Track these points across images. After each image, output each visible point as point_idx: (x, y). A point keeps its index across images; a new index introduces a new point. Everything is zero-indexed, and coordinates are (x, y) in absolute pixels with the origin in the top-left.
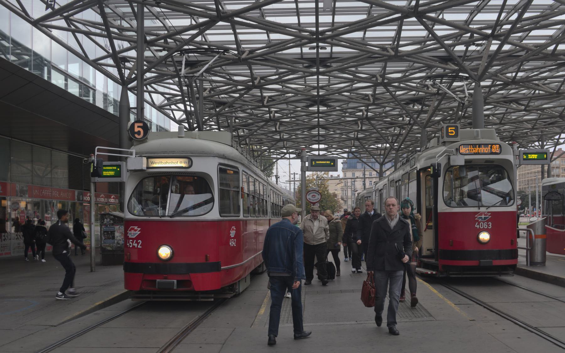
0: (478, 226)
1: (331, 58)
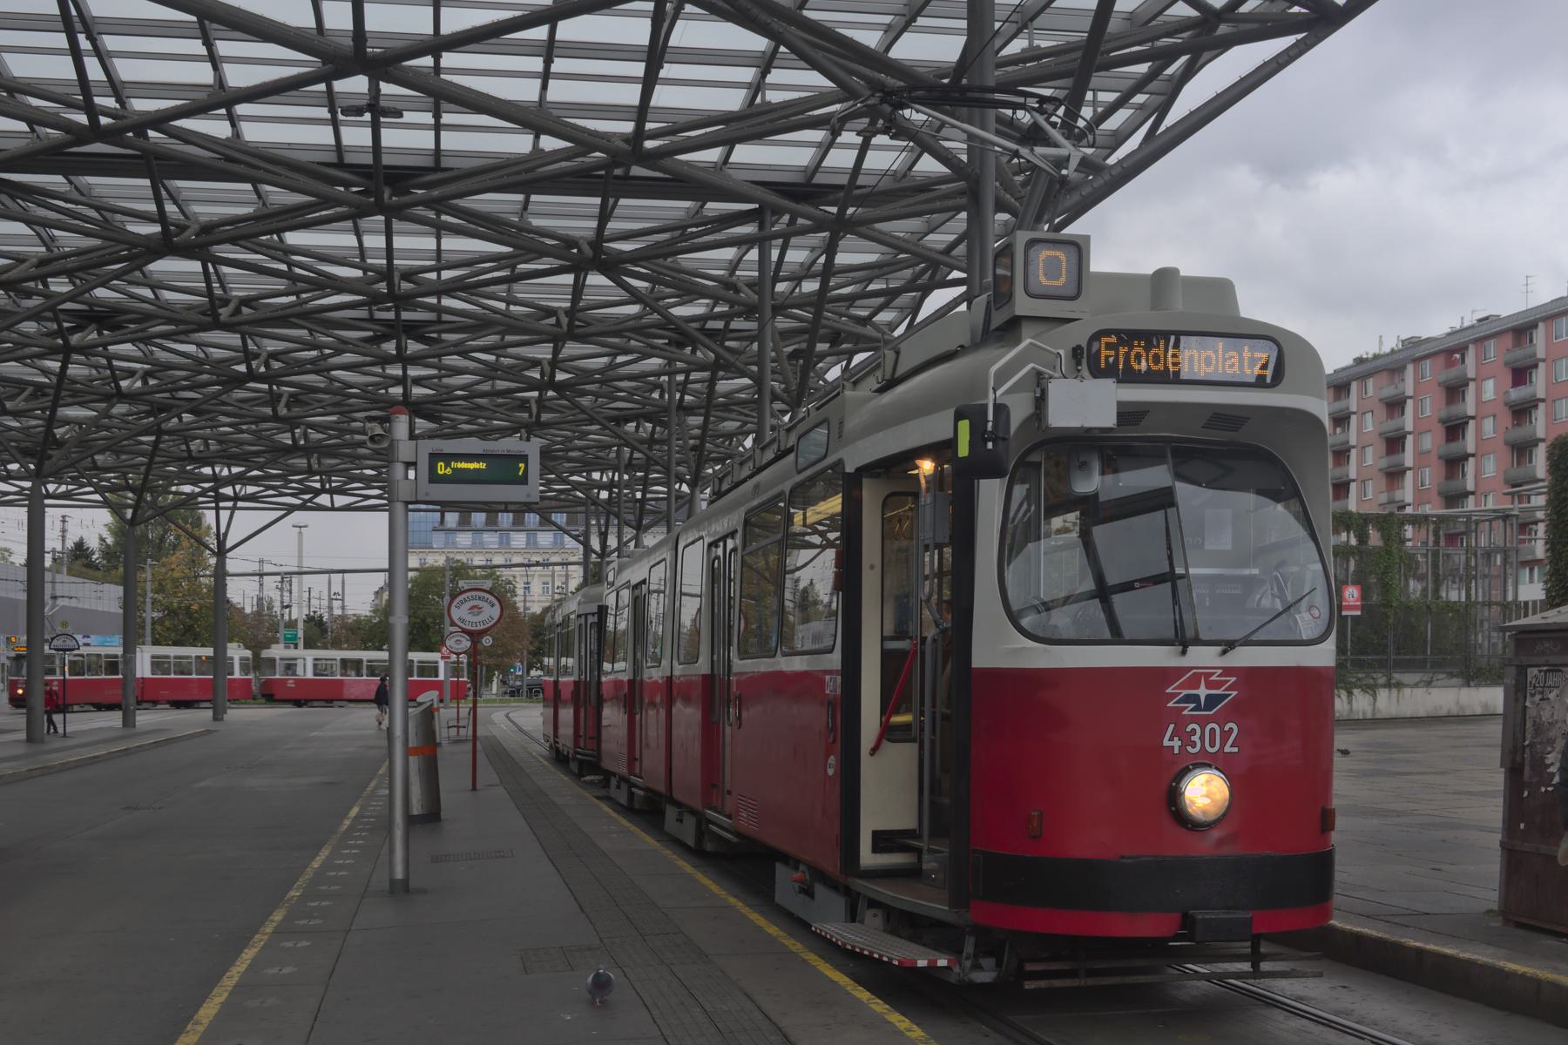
0: (1177, 743)
1: (437, 168)
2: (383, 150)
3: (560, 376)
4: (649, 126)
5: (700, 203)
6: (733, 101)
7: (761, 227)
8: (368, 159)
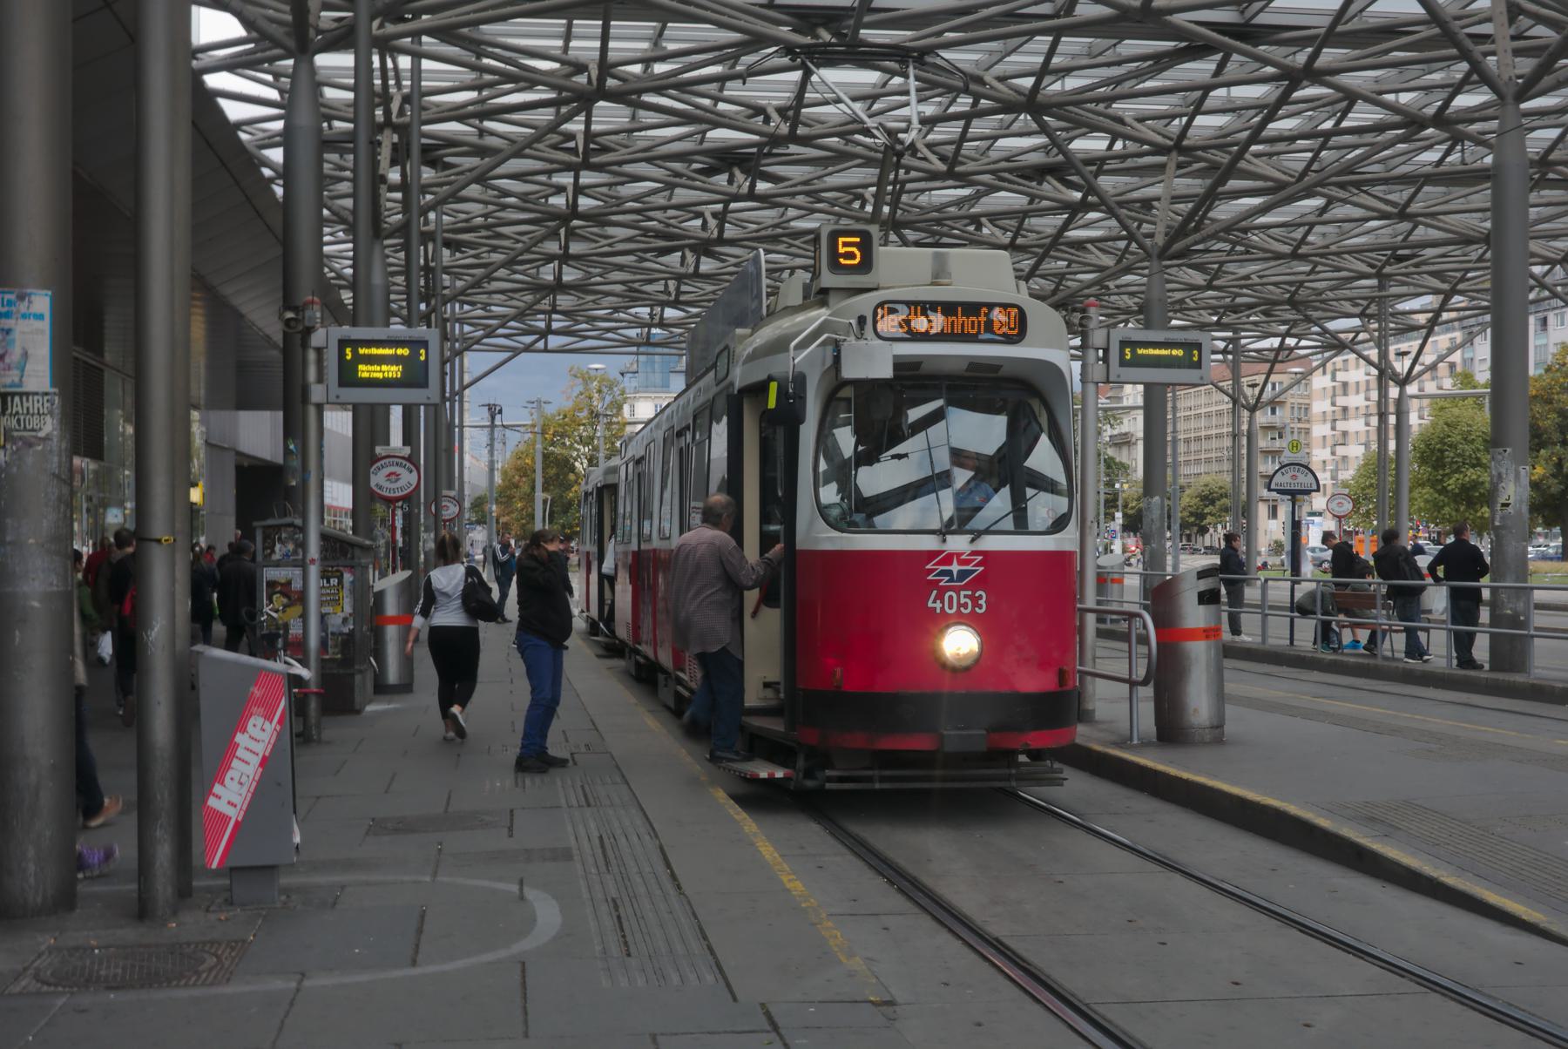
0: (938, 605)
3: (585, 203)
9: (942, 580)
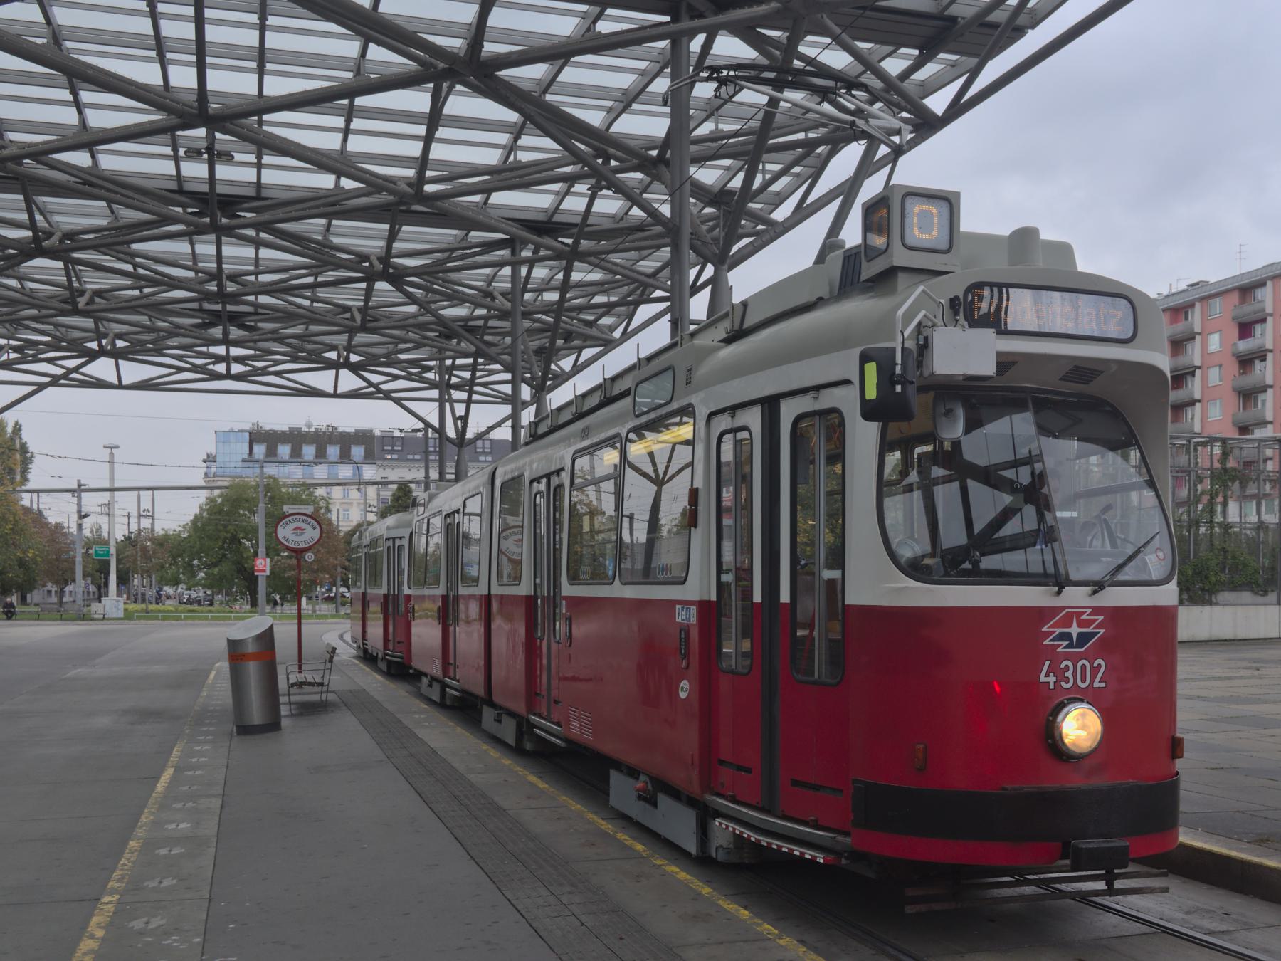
2: (217, 182)
4: (429, 174)
5: (465, 232)
6: (492, 158)
7: (513, 253)
8: (205, 188)
9: (1060, 645)
